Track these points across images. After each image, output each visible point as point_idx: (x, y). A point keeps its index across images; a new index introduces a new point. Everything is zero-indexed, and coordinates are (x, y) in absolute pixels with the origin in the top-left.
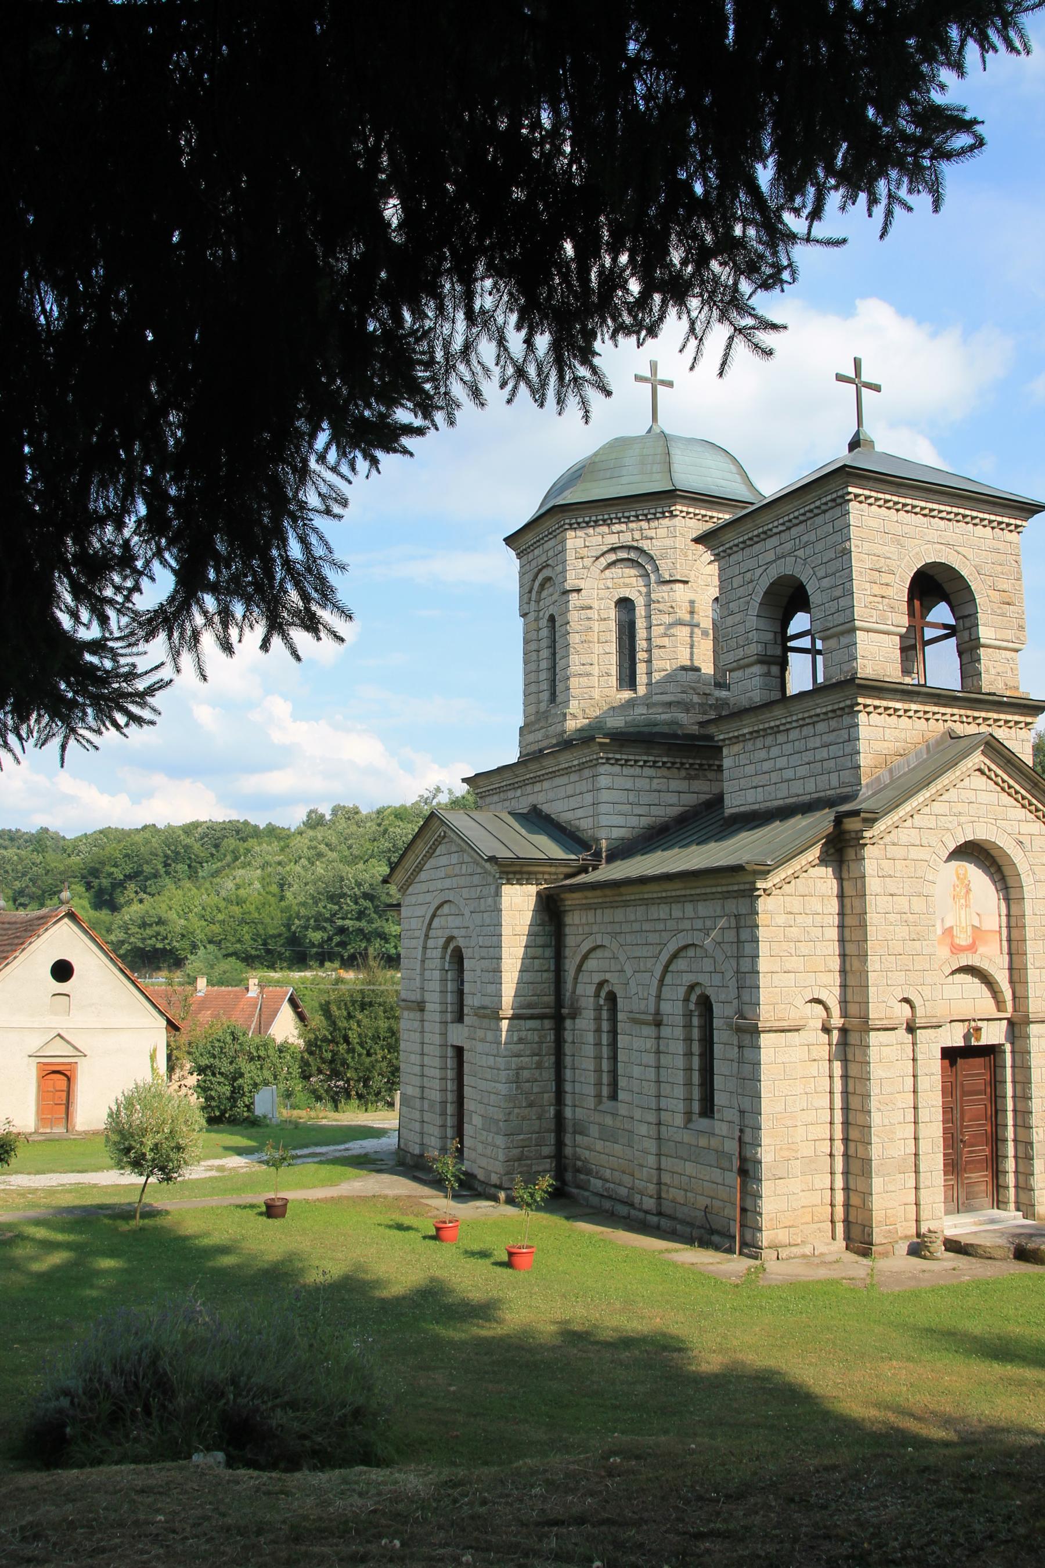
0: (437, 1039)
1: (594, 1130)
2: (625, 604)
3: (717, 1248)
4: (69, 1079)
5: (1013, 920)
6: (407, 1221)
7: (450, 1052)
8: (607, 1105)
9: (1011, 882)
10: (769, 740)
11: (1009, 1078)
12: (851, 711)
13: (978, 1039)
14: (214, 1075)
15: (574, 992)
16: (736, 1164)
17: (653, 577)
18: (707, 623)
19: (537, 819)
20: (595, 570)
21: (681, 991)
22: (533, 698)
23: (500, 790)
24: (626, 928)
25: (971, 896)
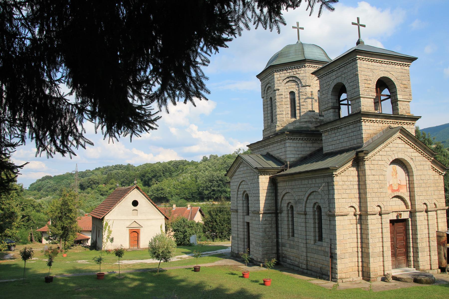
0: (242, 220)
1: (288, 245)
2: (292, 93)
3: (324, 279)
4: (138, 234)
5: (410, 182)
6: (234, 272)
7: (245, 224)
8: (291, 238)
9: (409, 170)
10: (336, 131)
11: (410, 228)
12: (360, 121)
13: (401, 217)
14: (178, 232)
15: (281, 206)
16: (329, 255)
17: (300, 85)
18: (316, 98)
19: (269, 156)
20: (283, 84)
21: (312, 205)
22: (266, 122)
23: (258, 148)
24: (295, 187)
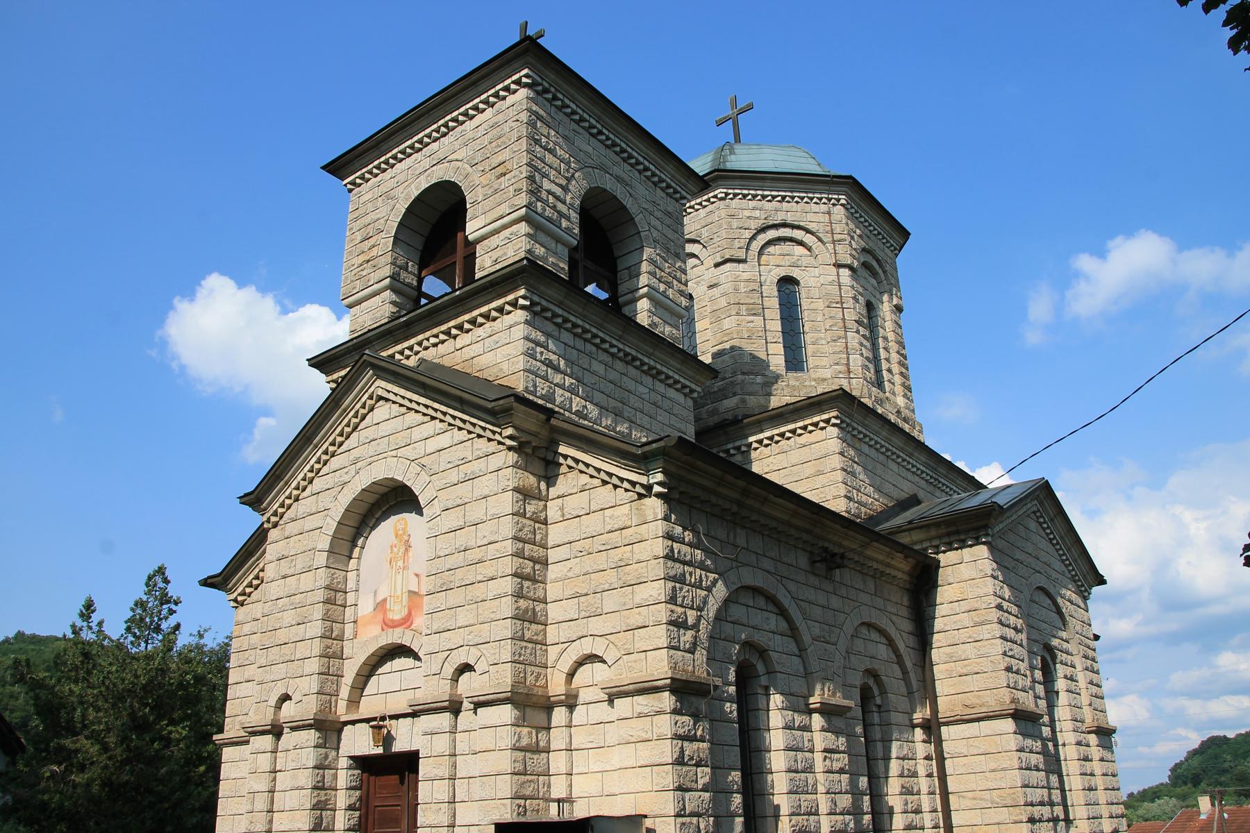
25: (410, 554)
